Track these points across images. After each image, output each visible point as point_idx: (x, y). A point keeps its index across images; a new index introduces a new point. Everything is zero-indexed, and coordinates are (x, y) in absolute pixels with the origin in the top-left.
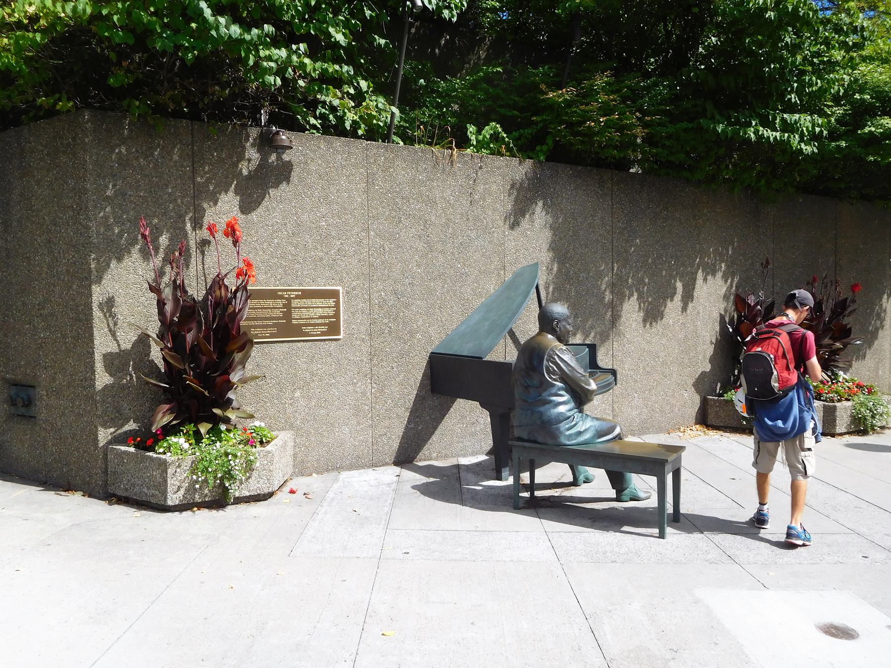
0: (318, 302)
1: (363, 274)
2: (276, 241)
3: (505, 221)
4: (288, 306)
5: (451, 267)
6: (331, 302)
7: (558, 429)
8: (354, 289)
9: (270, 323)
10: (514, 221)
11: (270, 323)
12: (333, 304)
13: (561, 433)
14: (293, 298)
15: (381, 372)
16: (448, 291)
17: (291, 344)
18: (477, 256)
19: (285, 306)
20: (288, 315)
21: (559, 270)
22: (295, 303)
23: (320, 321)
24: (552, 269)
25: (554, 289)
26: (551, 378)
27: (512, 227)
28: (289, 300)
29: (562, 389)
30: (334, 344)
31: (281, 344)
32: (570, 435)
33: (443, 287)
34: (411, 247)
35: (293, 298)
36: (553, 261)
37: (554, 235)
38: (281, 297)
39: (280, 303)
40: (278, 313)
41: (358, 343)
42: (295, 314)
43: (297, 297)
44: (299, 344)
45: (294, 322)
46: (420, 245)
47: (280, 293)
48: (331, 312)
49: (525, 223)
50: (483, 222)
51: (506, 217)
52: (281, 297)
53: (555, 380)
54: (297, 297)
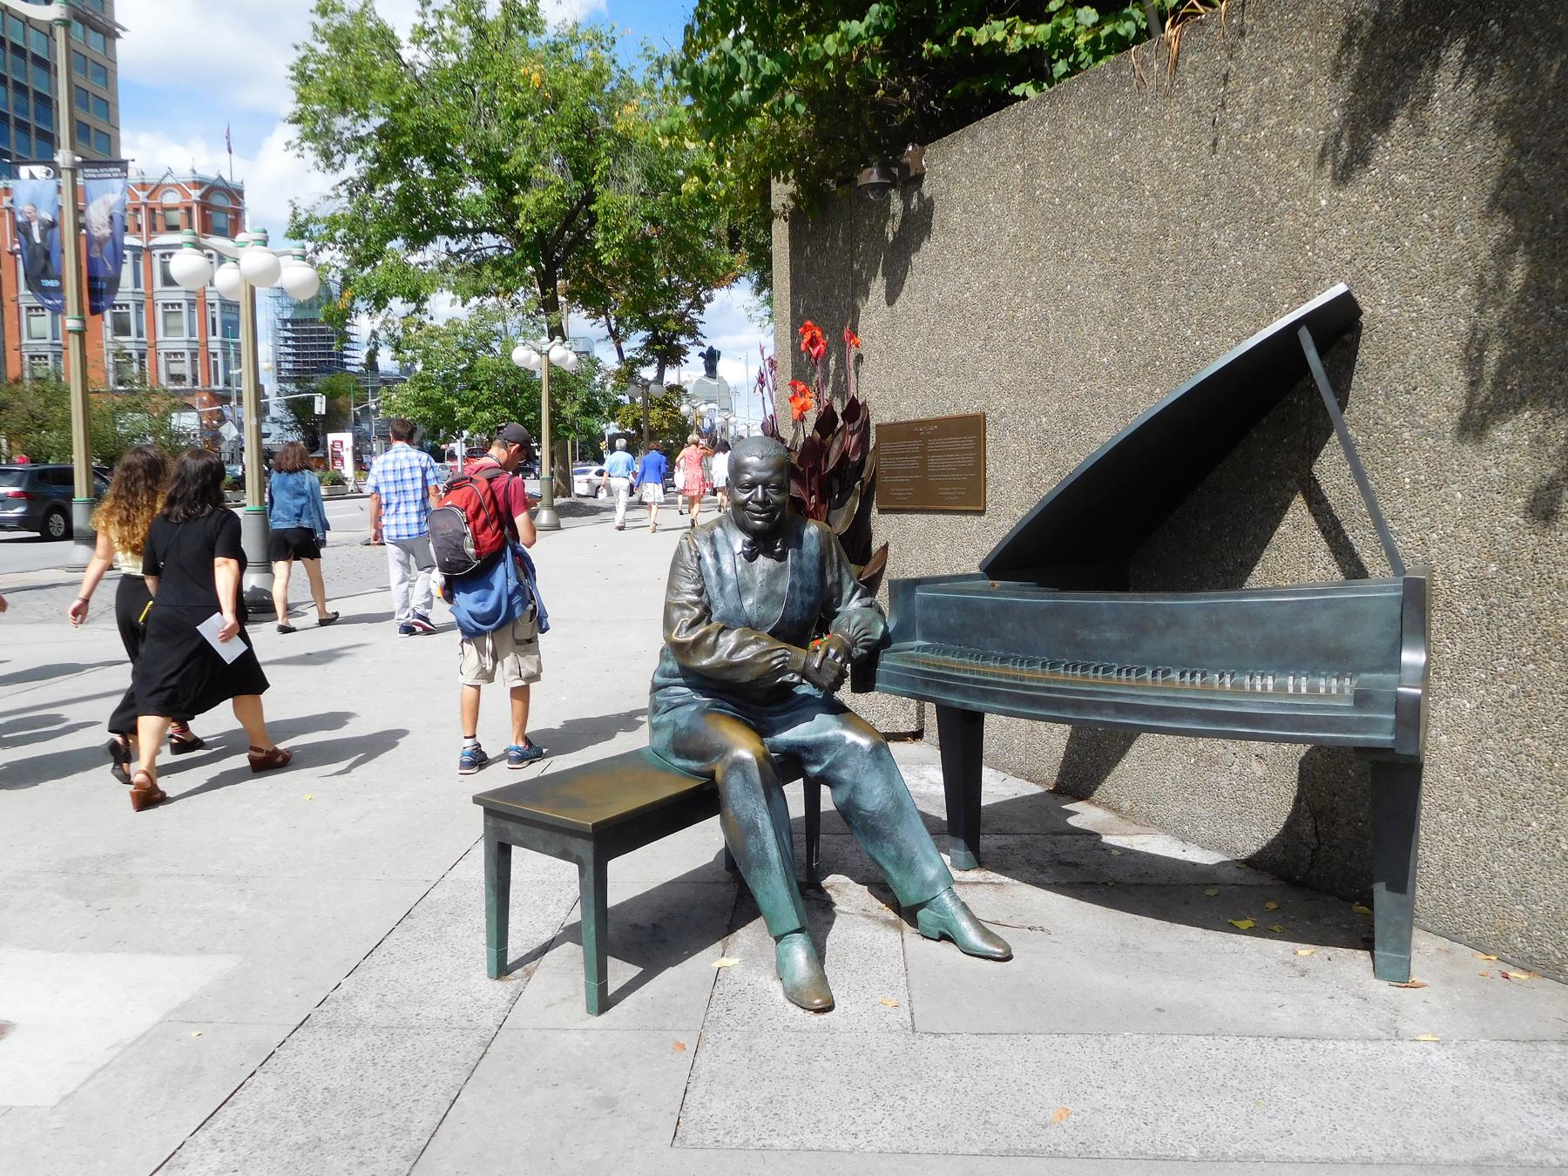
3: (1321, 164)
6: (968, 442)
8: (1003, 415)
10: (1350, 154)
12: (972, 445)
21: (1536, 288)
24: (1501, 284)
25: (1504, 365)
27: (1343, 177)
30: (977, 519)
33: (1151, 393)
34: (1091, 305)
35: (930, 437)
36: (1503, 253)
37: (1520, 148)
39: (915, 445)
40: (913, 463)
46: (1107, 298)
49: (1390, 150)
50: (1251, 193)
51: (1322, 156)
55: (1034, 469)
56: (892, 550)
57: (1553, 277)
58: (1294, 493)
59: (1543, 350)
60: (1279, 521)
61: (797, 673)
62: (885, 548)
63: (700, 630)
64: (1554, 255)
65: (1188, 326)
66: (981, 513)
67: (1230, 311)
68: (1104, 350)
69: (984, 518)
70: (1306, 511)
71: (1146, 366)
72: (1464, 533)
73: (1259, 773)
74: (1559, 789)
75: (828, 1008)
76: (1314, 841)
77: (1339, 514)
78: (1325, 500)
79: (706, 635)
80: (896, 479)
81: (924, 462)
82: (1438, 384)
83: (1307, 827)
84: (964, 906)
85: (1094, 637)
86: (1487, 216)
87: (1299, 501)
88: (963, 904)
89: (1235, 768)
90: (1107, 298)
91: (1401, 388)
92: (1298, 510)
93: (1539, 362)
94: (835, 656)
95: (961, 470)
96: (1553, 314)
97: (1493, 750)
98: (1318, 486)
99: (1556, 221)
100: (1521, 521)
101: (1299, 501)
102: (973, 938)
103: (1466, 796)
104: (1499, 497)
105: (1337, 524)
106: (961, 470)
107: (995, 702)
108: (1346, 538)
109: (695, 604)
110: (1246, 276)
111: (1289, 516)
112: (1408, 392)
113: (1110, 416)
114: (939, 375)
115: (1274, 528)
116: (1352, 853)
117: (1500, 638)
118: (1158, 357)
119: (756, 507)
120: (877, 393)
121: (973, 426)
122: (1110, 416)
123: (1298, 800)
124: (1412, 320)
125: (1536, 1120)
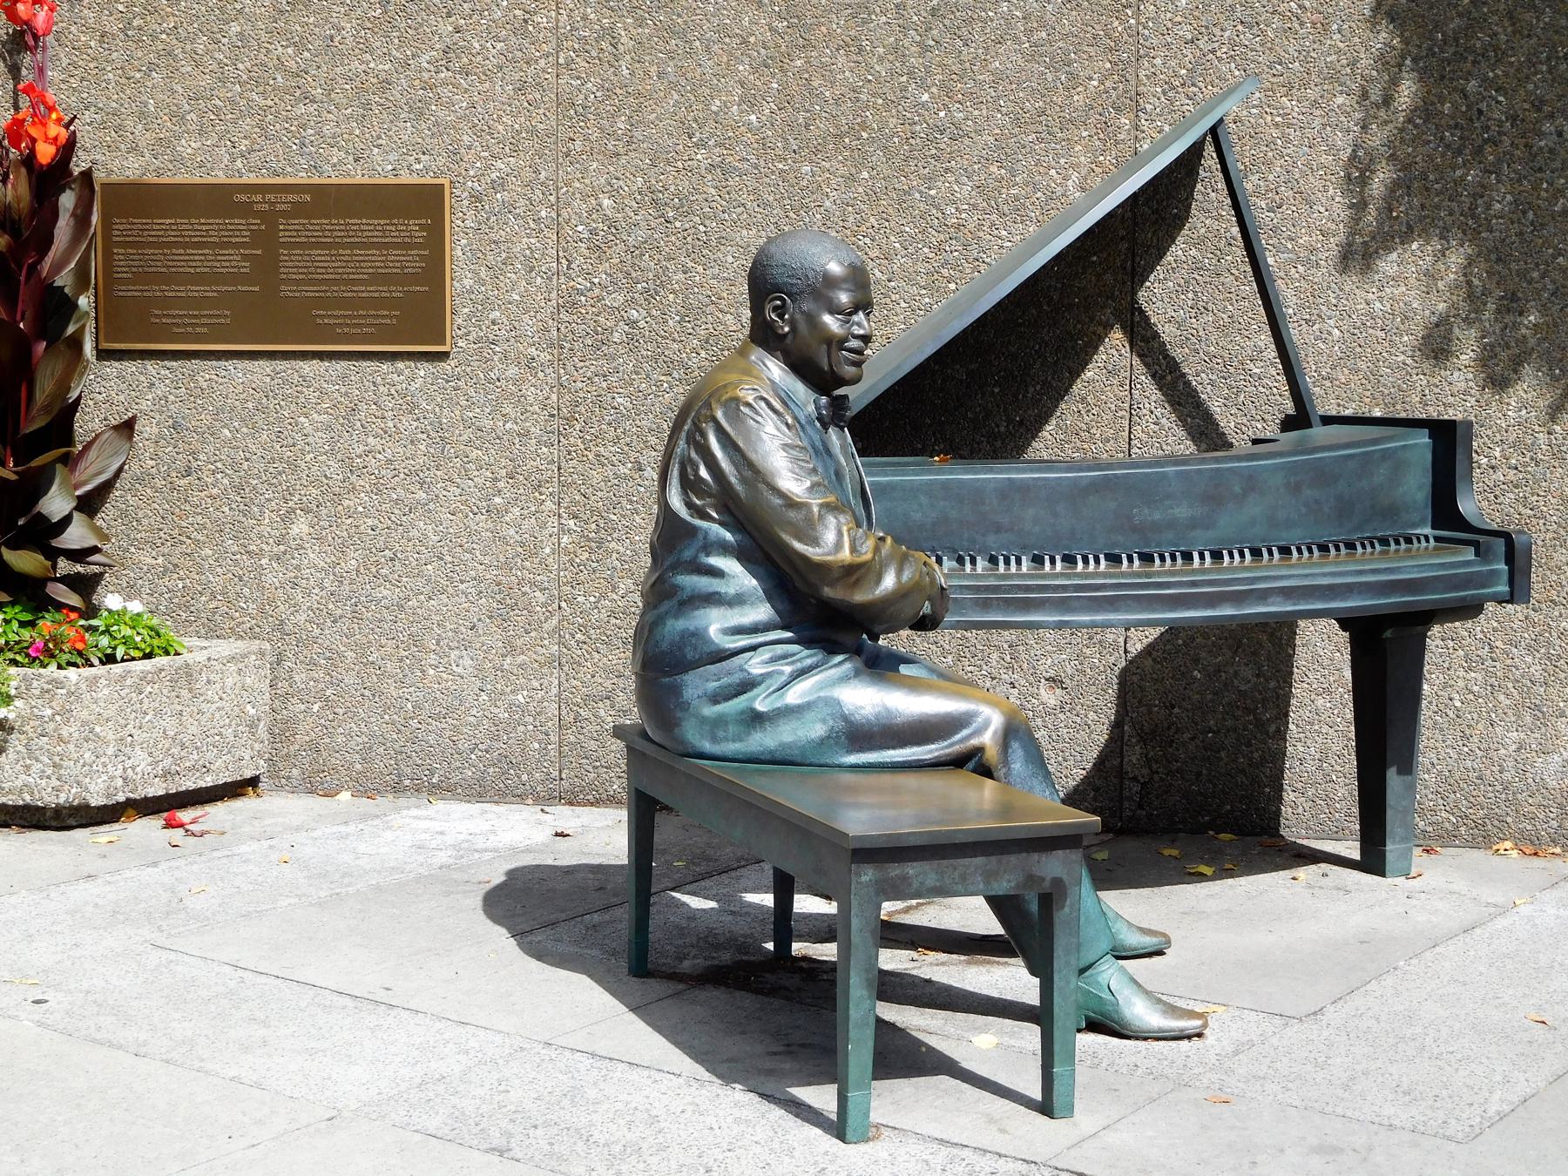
0: (369, 227)
1: (533, 131)
2: (235, 28)
4: (267, 240)
5: (888, 103)
6: (414, 228)
7: (676, 691)
8: (499, 185)
9: (210, 291)
11: (210, 291)
12: (420, 236)
13: (685, 707)
14: (283, 214)
15: (596, 476)
16: (873, 197)
17: (281, 365)
18: (1007, 59)
19: (257, 238)
20: (267, 268)
21: (1425, 110)
22: (288, 230)
23: (373, 291)
24: (1387, 101)
25: (1395, 186)
26: (689, 505)
28: (270, 218)
29: (724, 549)
30: (423, 370)
31: (248, 364)
32: (719, 722)
33: (852, 178)
34: (723, 31)
36: (1391, 66)
38: (246, 210)
39: (241, 228)
40: (232, 261)
41: (512, 371)
42: (291, 264)
43: (298, 210)
44: (307, 367)
45: (286, 290)
48: (413, 262)
52: (246, 210)
53: (704, 516)
54: (298, 210)
56: (145, 429)
57: (1442, 100)
58: (1108, 327)
59: (1431, 177)
60: (1083, 366)
62: (127, 428)
64: (1442, 77)
66: (444, 356)
68: (750, 102)
69: (447, 367)
70: (1126, 351)
71: (841, 136)
73: (1052, 702)
74: (1451, 644)
76: (1145, 771)
77: (1177, 353)
78: (1156, 335)
80: (181, 291)
82: (1311, 205)
83: (1134, 755)
85: (1157, 516)
86: (1373, 22)
87: (1117, 337)
92: (1115, 348)
93: (1427, 189)
95: (376, 278)
96: (1442, 138)
98: (1147, 319)
99: (1445, 41)
100: (1409, 361)
101: (1117, 337)
105: (1173, 366)
106: (376, 278)
107: (1116, 610)
108: (1188, 383)
110: (1029, 32)
111: (1100, 357)
114: (308, 98)
115: (1076, 373)
116: (1199, 774)
121: (425, 203)
122: (767, 205)
123: (1117, 726)
124: (1277, 125)
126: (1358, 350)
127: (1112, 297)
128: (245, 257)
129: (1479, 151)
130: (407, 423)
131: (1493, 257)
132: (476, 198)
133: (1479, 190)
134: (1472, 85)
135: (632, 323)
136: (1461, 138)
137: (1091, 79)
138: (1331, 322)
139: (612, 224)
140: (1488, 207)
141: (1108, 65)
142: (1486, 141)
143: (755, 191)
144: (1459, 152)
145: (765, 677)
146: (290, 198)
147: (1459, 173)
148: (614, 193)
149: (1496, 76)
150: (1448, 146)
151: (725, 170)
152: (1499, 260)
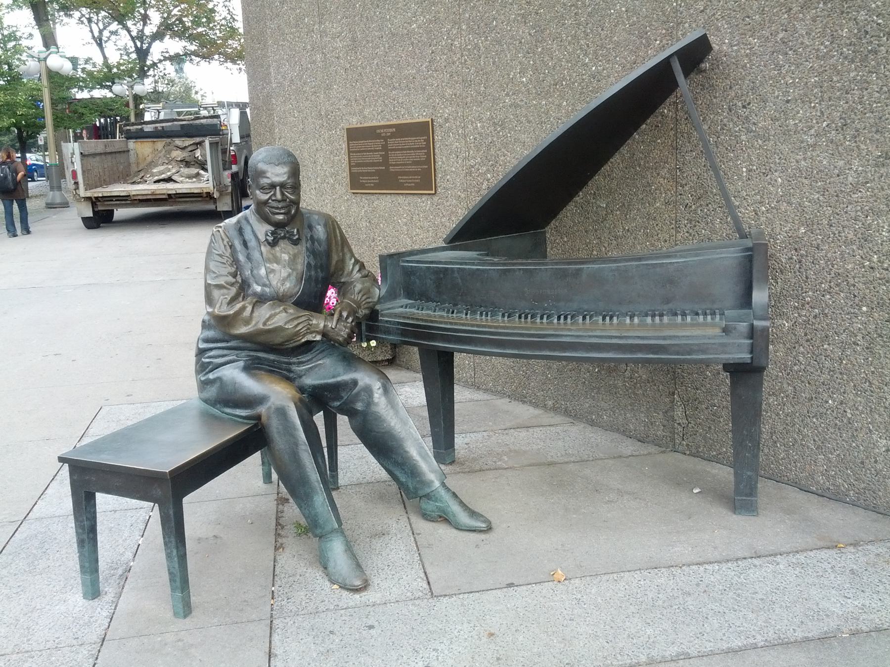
6: (420, 141)
20: (385, 161)
28: (385, 139)
33: (560, 105)
34: (512, 37)
35: (390, 137)
38: (379, 136)
39: (379, 143)
40: (377, 157)
43: (393, 135)
45: (391, 169)
46: (524, 32)
47: (378, 131)
48: (421, 155)
52: (379, 136)
54: (393, 135)
55: (472, 162)
57: (841, 26)
59: (835, 79)
61: (318, 333)
63: (239, 306)
64: (842, 13)
65: (586, 55)
67: (618, 44)
68: (523, 72)
69: (436, 198)
72: (784, 206)
75: (365, 587)
76: (685, 421)
79: (243, 308)
81: (386, 158)
82: (765, 101)
84: (455, 495)
88: (454, 493)
89: (628, 374)
90: (524, 32)
91: (740, 104)
93: (833, 87)
94: (347, 318)
97: (802, 353)
100: (821, 198)
102: (464, 518)
103: (785, 385)
104: (806, 182)
109: (232, 285)
110: (628, 18)
112: (744, 107)
113: (529, 122)
114: (394, 88)
116: (710, 428)
117: (807, 278)
118: (564, 79)
119: (275, 204)
120: (345, 102)
121: (423, 129)
122: (529, 122)
124: (747, 55)
125: (849, 601)
126: (792, 191)
127: (666, 162)
128: (381, 156)
129: (864, 59)
130: (426, 224)
131: (874, 129)
132: (441, 126)
133: (865, 85)
134: (862, 16)
135: (488, 180)
136: (853, 52)
137: (656, 40)
138: (777, 174)
139: (480, 134)
140: (871, 95)
141: (664, 31)
142: (870, 52)
143: (526, 116)
144: (853, 61)
145: (209, 363)
146: (391, 130)
147: (852, 75)
148: (480, 120)
149: (878, 7)
150: (846, 58)
151: (516, 106)
152: (877, 131)
